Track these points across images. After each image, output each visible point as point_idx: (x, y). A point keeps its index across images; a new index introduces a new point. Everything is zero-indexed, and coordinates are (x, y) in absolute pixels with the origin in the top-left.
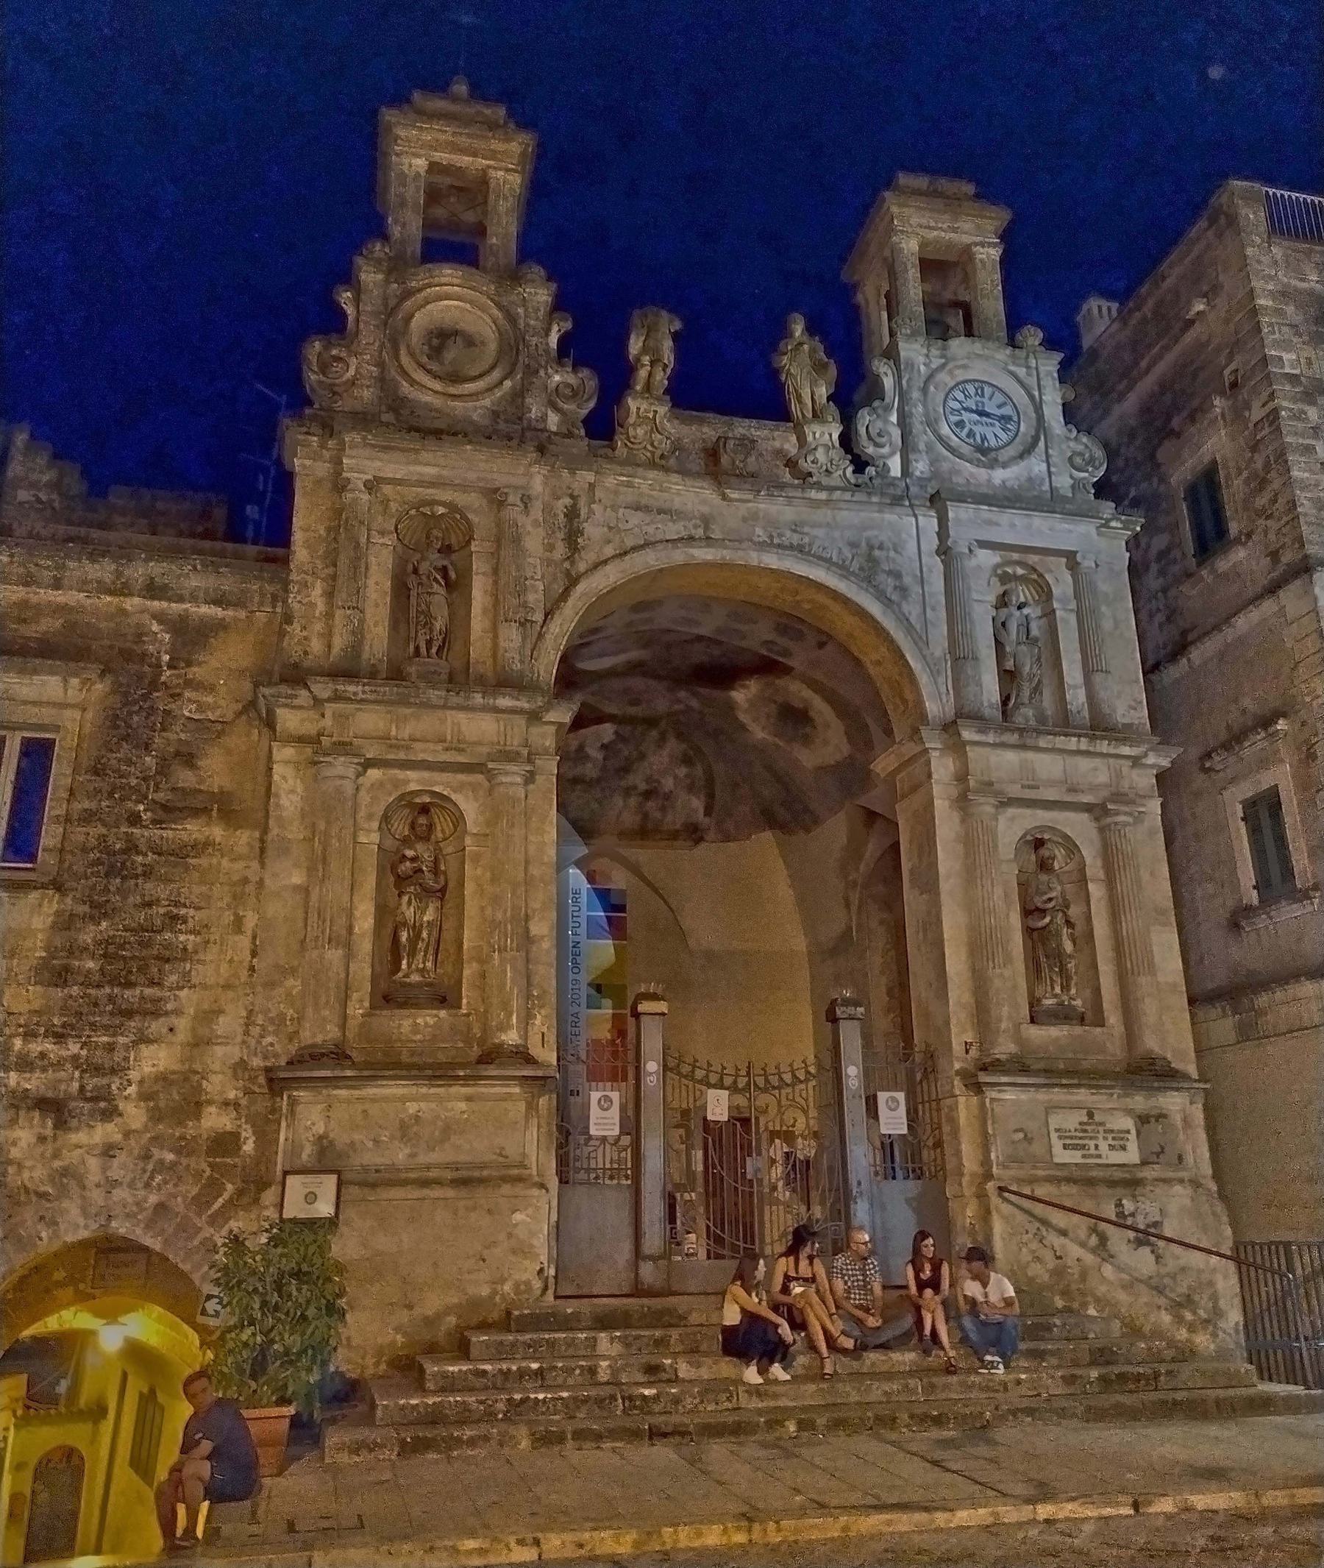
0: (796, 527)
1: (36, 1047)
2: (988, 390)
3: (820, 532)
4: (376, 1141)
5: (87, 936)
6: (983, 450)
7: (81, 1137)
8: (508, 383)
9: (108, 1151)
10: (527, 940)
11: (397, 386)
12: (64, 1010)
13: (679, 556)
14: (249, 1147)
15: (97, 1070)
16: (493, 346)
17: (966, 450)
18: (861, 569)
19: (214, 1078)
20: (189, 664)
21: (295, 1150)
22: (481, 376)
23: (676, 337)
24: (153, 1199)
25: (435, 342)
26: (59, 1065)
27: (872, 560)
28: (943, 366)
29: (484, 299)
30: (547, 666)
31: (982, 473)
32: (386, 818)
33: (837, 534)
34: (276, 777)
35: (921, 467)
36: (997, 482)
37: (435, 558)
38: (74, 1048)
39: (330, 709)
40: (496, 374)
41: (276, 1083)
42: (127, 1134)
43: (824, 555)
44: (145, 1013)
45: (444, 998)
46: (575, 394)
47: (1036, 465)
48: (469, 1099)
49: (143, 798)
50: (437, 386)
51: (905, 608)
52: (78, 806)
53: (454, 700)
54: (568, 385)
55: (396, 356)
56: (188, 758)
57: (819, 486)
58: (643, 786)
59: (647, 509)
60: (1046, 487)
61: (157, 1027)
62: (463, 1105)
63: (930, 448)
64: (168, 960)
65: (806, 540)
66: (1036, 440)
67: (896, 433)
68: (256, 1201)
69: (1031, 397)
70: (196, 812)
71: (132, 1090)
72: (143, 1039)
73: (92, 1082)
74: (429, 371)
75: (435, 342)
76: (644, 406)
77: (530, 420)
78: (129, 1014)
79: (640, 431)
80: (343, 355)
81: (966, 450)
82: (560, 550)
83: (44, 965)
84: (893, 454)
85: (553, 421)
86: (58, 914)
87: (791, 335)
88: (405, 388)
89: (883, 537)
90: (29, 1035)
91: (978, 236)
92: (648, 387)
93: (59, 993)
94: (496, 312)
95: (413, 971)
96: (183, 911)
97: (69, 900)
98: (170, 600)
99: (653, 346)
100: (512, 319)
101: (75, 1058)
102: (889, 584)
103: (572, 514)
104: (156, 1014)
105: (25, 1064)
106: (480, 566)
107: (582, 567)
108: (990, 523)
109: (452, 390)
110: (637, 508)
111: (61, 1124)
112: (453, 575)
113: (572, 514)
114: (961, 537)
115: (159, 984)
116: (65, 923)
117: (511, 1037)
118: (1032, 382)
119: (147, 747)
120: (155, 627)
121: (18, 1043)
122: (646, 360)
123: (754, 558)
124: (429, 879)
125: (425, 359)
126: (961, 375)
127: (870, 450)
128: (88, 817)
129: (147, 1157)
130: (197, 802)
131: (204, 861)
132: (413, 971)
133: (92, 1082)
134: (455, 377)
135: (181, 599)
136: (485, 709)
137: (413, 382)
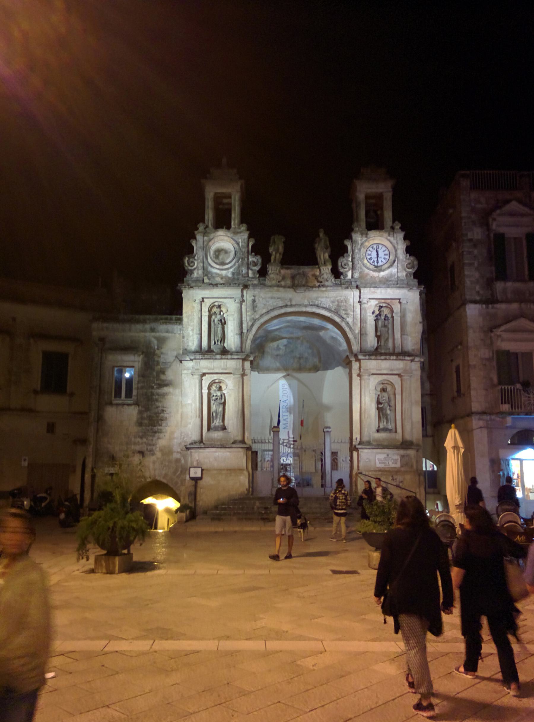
0: (317, 298)
2: (380, 246)
3: (323, 300)
5: (145, 415)
6: (376, 267)
9: (154, 463)
11: (207, 268)
15: (150, 445)
18: (335, 309)
21: (192, 462)
24: (164, 472)
25: (217, 253)
28: (366, 241)
31: (376, 274)
33: (328, 300)
35: (356, 275)
36: (380, 276)
38: (144, 440)
39: (194, 361)
40: (234, 261)
42: (158, 459)
43: (325, 306)
44: (159, 432)
47: (394, 270)
48: (230, 452)
49: (154, 383)
50: (218, 267)
51: (348, 319)
52: (140, 385)
53: (223, 357)
54: (254, 262)
55: (207, 259)
56: (163, 372)
57: (323, 286)
58: (298, 356)
59: (275, 298)
60: (396, 277)
61: (161, 435)
62: (228, 453)
64: (163, 420)
65: (320, 302)
66: (394, 261)
67: (350, 264)
68: (185, 473)
69: (394, 247)
70: (166, 385)
71: (158, 449)
72: (159, 438)
73: (149, 448)
74: (216, 263)
75: (217, 253)
76: (273, 267)
77: (242, 274)
78: (156, 432)
80: (193, 260)
81: (372, 267)
84: (349, 270)
86: (139, 410)
87: (319, 236)
88: (210, 269)
89: (342, 299)
90: (135, 437)
91: (384, 189)
92: (275, 260)
93: (140, 428)
94: (233, 242)
95: (217, 422)
96: (165, 409)
97: (140, 407)
98: (155, 332)
101: (145, 442)
102: (342, 313)
104: (161, 432)
105: (135, 444)
107: (257, 317)
108: (374, 292)
110: (272, 298)
111: (143, 456)
112: (223, 321)
115: (161, 426)
116: (140, 412)
118: (395, 242)
119: (154, 370)
120: (153, 339)
121: (133, 439)
122: (274, 253)
125: (214, 259)
126: (372, 242)
127: (342, 270)
128: (142, 388)
129: (162, 463)
130: (166, 382)
132: (217, 422)
133: (149, 448)
134: (223, 264)
135: (158, 332)
136: (231, 359)
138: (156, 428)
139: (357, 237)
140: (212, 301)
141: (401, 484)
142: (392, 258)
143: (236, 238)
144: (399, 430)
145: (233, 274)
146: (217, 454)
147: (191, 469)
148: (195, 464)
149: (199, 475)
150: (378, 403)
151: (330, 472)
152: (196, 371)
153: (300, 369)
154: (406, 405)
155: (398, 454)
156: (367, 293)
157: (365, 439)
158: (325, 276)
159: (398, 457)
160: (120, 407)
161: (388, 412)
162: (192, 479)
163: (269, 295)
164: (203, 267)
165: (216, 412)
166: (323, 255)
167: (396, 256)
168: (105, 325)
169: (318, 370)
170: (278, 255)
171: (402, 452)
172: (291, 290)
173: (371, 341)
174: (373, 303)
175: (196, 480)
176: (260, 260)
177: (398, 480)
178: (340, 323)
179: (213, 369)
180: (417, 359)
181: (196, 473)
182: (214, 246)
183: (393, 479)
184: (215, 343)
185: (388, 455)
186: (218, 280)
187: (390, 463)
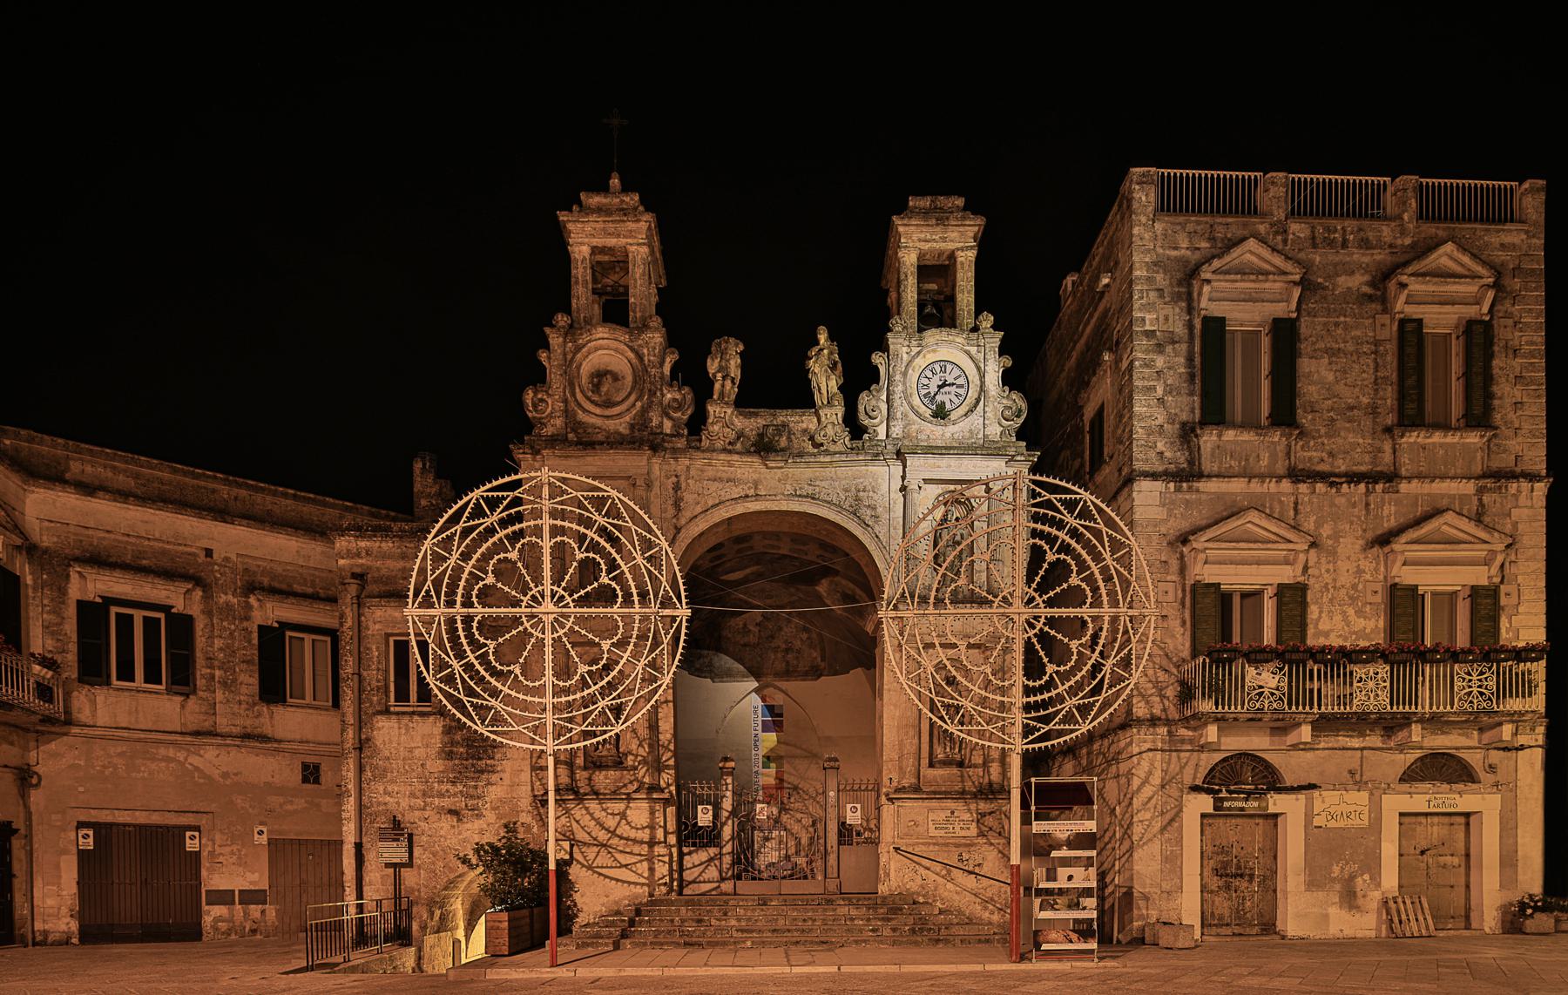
1: (444, 787)
5: (458, 737)
7: (469, 826)
8: (639, 404)
11: (575, 414)
12: (453, 771)
13: (740, 509)
16: (629, 379)
23: (742, 354)
26: (455, 795)
27: (858, 499)
29: (623, 347)
46: (680, 406)
50: (598, 411)
54: (675, 400)
55: (573, 395)
57: (827, 452)
59: (721, 480)
61: (494, 778)
72: (489, 784)
73: (470, 803)
78: (482, 772)
79: (716, 428)
82: (671, 511)
83: (442, 750)
85: (668, 426)
88: (581, 416)
92: (722, 394)
94: (631, 355)
99: (726, 364)
100: (640, 357)
103: (677, 487)
105: (441, 795)
107: (683, 521)
109: (608, 412)
111: (459, 820)
113: (677, 487)
114: (913, 482)
123: (785, 506)
134: (609, 404)
137: (585, 411)
138: (482, 763)
139: (899, 343)
145: (632, 427)
156: (919, 466)
158: (830, 431)
160: (405, 720)
164: (566, 411)
166: (825, 379)
168: (363, 544)
170: (728, 383)
172: (756, 459)
176: (689, 397)
178: (861, 537)
182: (589, 364)
186: (600, 437)
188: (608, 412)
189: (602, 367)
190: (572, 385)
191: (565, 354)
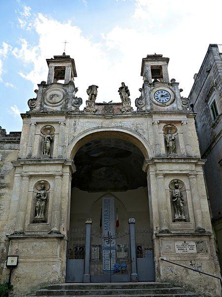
4: (27, 250)
10: (61, 209)
14: (5, 251)
17: (159, 103)
19: (3, 238)
20: (4, 160)
22: (59, 102)
30: (68, 155)
32: (35, 187)
34: (15, 180)
37: (49, 136)
40: (62, 101)
41: (10, 239)
45: (45, 221)
47: (174, 105)
48: (46, 242)
50: (51, 105)
62: (45, 243)
63: (151, 104)
66: (174, 101)
67: (144, 102)
70: (3, 187)
88: (45, 106)
100: (66, 91)
106: (56, 136)
107: (76, 135)
113: (75, 124)
117: (55, 229)
118: (173, 89)
123: (111, 130)
124: (43, 198)
126: (158, 89)
130: (4, 186)
131: (4, 196)
140: (44, 125)
141: (199, 269)
142: (172, 98)
143: (65, 88)
144: (192, 220)
146: (35, 243)
147: (9, 257)
148: (14, 253)
149: (15, 264)
150: (173, 198)
151: (135, 258)
152: (25, 174)
153: (116, 189)
154: (196, 199)
155: (193, 241)
157: (164, 228)
159: (194, 244)
161: (182, 205)
162: (8, 267)
163: (86, 120)
165: (40, 207)
167: (175, 96)
169: (127, 190)
171: (197, 239)
173: (163, 150)
174: (163, 125)
175: (12, 268)
177: (196, 265)
179: (38, 172)
180: (199, 163)
181: (12, 261)
183: (192, 265)
184: (44, 154)
185: (185, 242)
187: (188, 249)
188: (54, 105)
189: (54, 94)
190: (44, 98)
191: (43, 90)
